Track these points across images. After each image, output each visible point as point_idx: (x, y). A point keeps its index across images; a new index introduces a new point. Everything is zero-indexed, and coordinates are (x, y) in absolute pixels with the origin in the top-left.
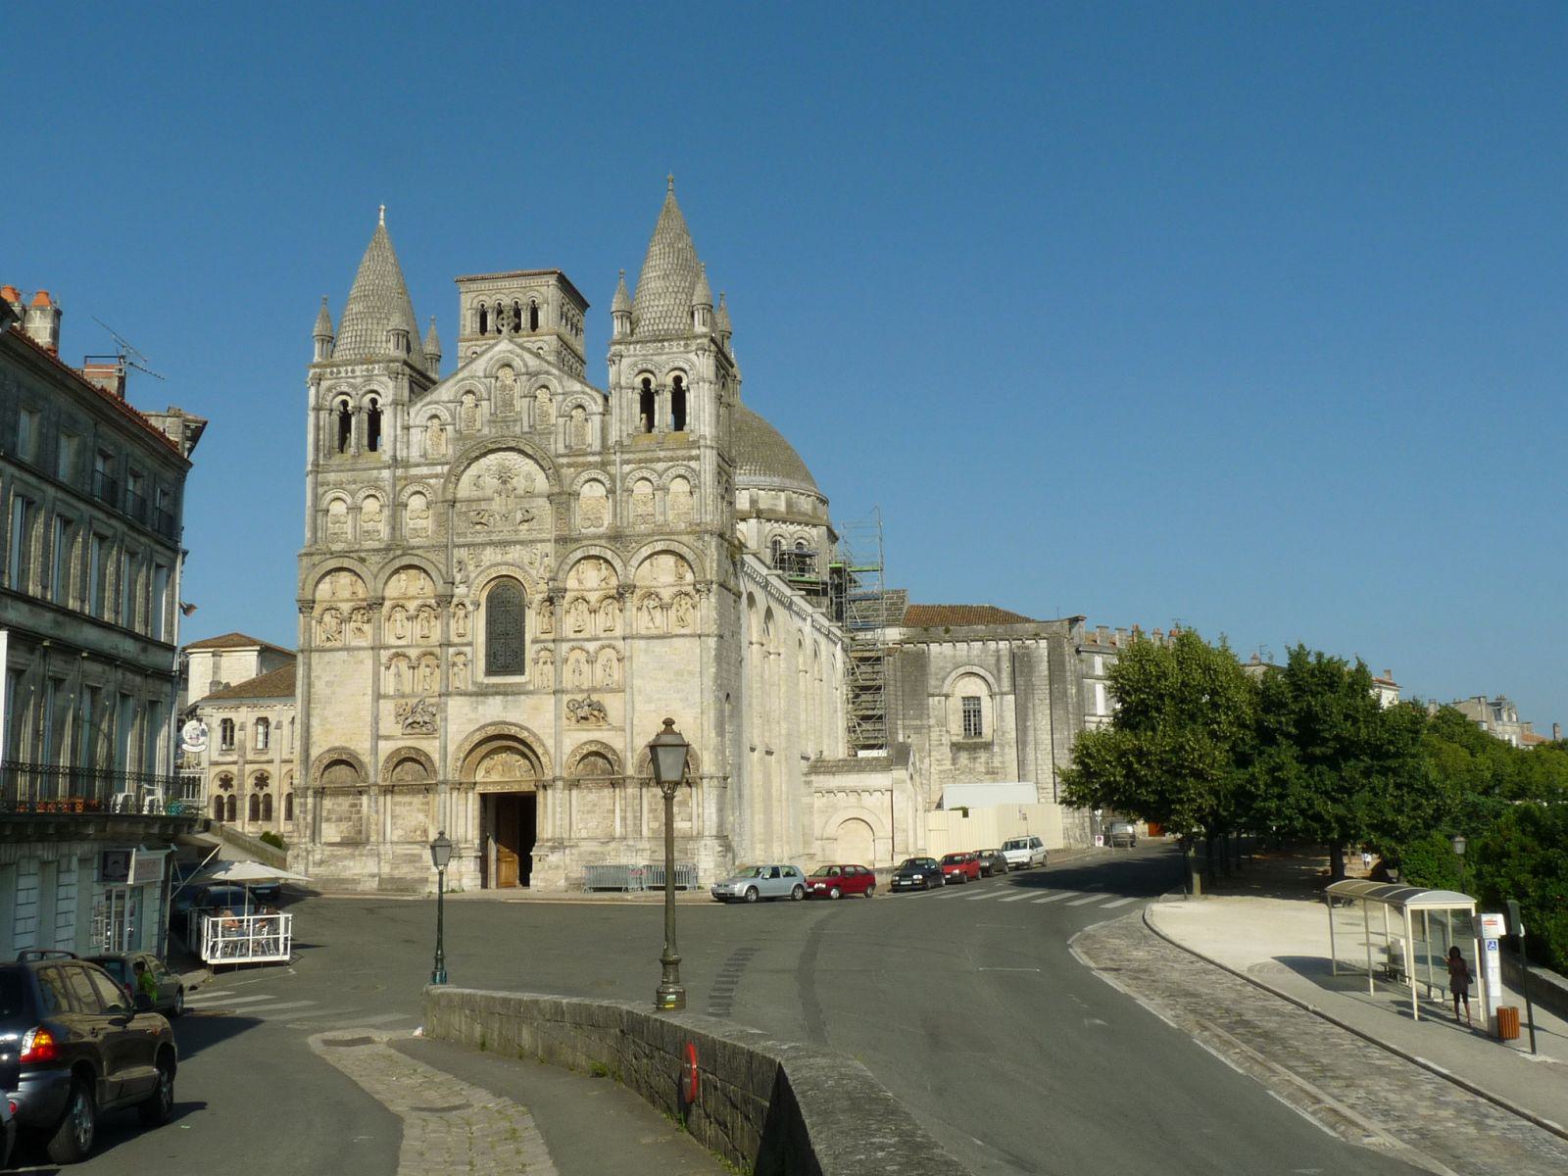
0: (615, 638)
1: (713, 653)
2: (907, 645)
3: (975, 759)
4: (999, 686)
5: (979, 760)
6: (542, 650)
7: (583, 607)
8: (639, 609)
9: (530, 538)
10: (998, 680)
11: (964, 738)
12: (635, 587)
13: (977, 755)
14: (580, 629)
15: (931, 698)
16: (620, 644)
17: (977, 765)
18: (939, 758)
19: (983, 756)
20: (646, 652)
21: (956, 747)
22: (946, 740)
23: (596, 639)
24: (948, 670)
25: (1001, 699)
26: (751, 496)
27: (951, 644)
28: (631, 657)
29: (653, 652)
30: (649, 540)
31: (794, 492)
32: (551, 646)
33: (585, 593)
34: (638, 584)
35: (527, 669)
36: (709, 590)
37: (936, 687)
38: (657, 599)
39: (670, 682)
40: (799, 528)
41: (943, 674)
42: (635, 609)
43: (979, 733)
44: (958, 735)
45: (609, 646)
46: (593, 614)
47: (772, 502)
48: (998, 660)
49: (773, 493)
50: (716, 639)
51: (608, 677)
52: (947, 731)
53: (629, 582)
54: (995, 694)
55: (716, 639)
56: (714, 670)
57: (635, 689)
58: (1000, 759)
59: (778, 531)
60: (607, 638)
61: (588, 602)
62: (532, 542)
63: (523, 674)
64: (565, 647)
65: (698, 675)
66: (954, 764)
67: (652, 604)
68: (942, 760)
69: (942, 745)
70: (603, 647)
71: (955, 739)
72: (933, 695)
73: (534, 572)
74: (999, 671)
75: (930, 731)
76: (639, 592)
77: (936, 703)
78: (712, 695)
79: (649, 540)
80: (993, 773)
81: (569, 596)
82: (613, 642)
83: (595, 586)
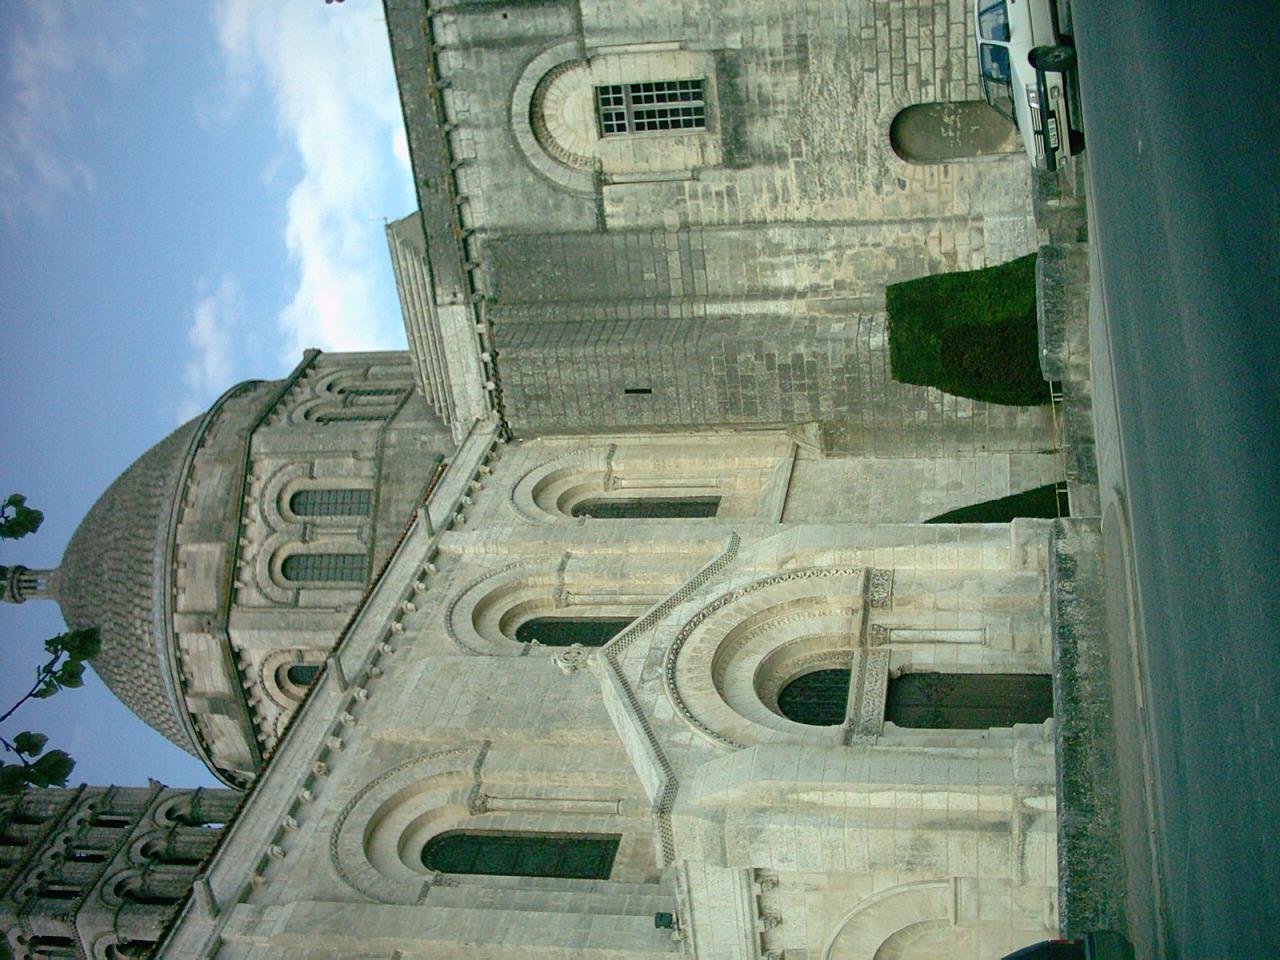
2: (479, 285)
3: (764, 101)
4: (560, 38)
5: (768, 89)
10: (541, 41)
11: (711, 130)
13: (754, 97)
15: (611, 223)
17: (781, 94)
18: (766, 197)
19: (756, 78)
21: (737, 152)
22: (717, 182)
24: (531, 179)
25: (593, 32)
26: (190, 630)
27: (461, 173)
31: (179, 521)
37: (579, 210)
40: (254, 510)
41: (542, 192)
43: (694, 88)
44: (703, 146)
47: (201, 574)
48: (490, 44)
49: (181, 572)
52: (695, 179)
54: (582, 49)
58: (761, 30)
59: (261, 567)
66: (780, 158)
68: (772, 189)
69: (730, 192)
71: (714, 155)
72: (601, 215)
74: (518, 41)
75: (697, 224)
77: (620, 209)
80: (802, 47)
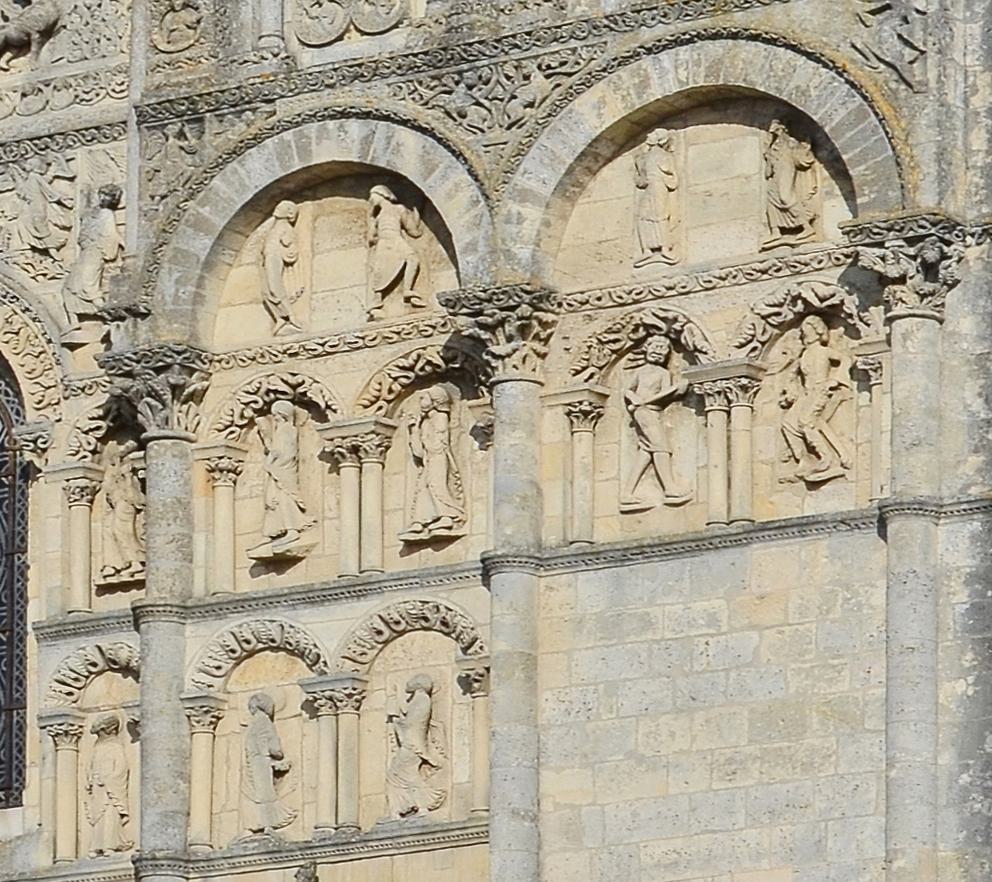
0: (451, 574)
1: (960, 597)
6: (93, 671)
7: (284, 430)
8: (588, 414)
9: (40, 125)
12: (542, 298)
14: (280, 547)
16: (468, 602)
20: (611, 627)
23: (357, 588)
28: (530, 663)
29: (647, 624)
30: (617, 45)
32: (125, 644)
33: (305, 368)
34: (565, 288)
35: (32, 775)
36: (930, 270)
38: (677, 359)
39: (732, 767)
42: (553, 422)
45: (422, 622)
46: (348, 471)
50: (976, 525)
51: (412, 772)
53: (512, 275)
55: (976, 525)
56: (963, 687)
57: (551, 819)
60: (402, 580)
61: (319, 412)
62: (42, 143)
63: (21, 805)
64: (202, 642)
65: (874, 723)
67: (653, 381)
70: (393, 630)
73: (49, 294)
76: (574, 332)
78: (951, 818)
79: (617, 45)
81: (225, 392)
82: (442, 597)
83: (350, 320)
